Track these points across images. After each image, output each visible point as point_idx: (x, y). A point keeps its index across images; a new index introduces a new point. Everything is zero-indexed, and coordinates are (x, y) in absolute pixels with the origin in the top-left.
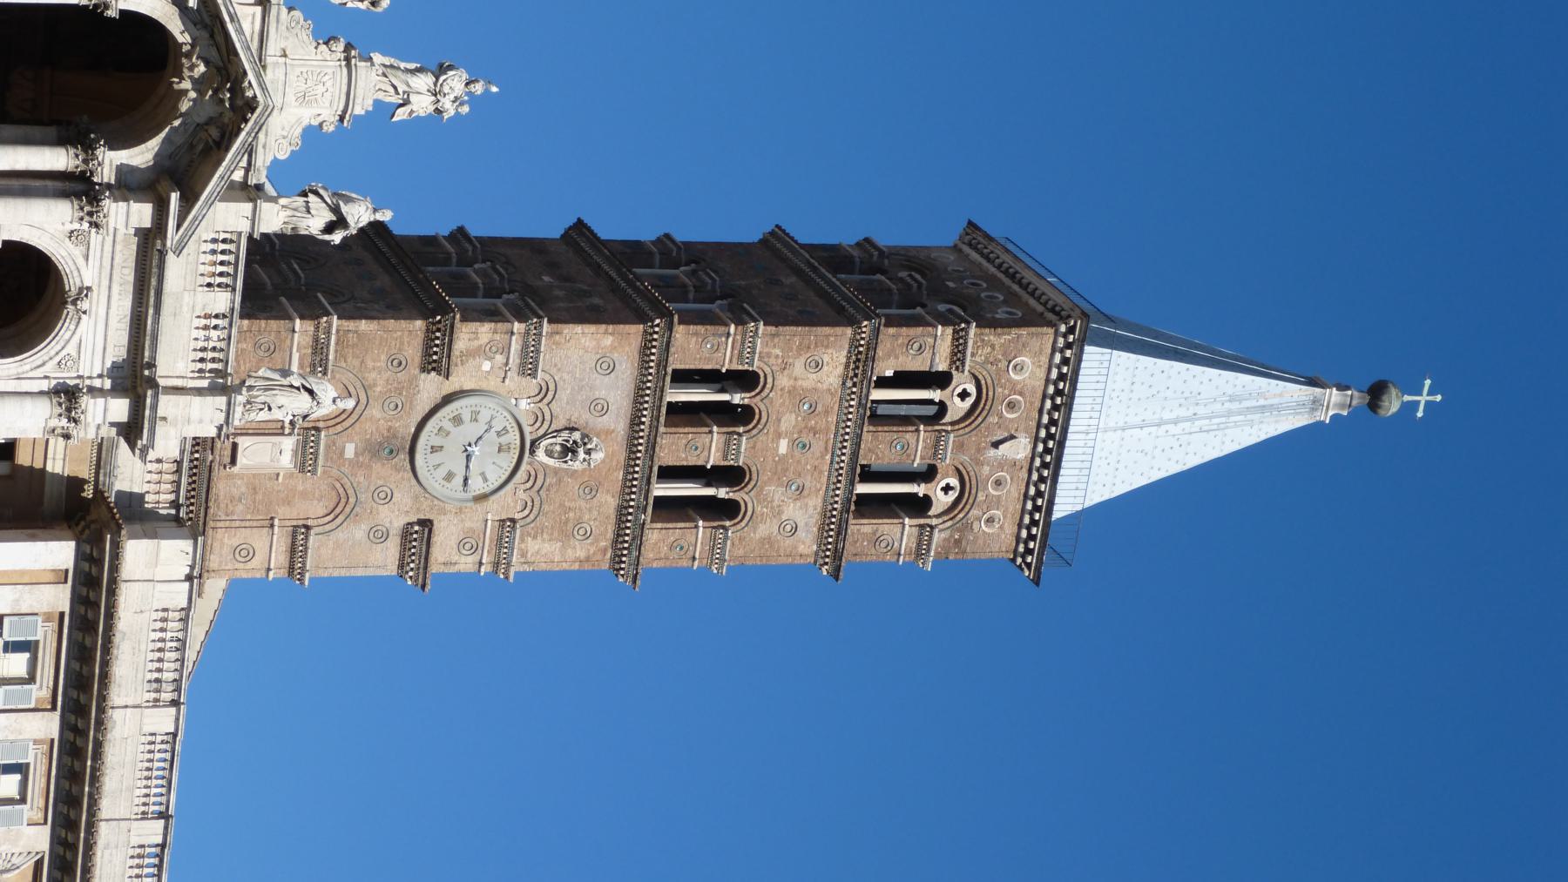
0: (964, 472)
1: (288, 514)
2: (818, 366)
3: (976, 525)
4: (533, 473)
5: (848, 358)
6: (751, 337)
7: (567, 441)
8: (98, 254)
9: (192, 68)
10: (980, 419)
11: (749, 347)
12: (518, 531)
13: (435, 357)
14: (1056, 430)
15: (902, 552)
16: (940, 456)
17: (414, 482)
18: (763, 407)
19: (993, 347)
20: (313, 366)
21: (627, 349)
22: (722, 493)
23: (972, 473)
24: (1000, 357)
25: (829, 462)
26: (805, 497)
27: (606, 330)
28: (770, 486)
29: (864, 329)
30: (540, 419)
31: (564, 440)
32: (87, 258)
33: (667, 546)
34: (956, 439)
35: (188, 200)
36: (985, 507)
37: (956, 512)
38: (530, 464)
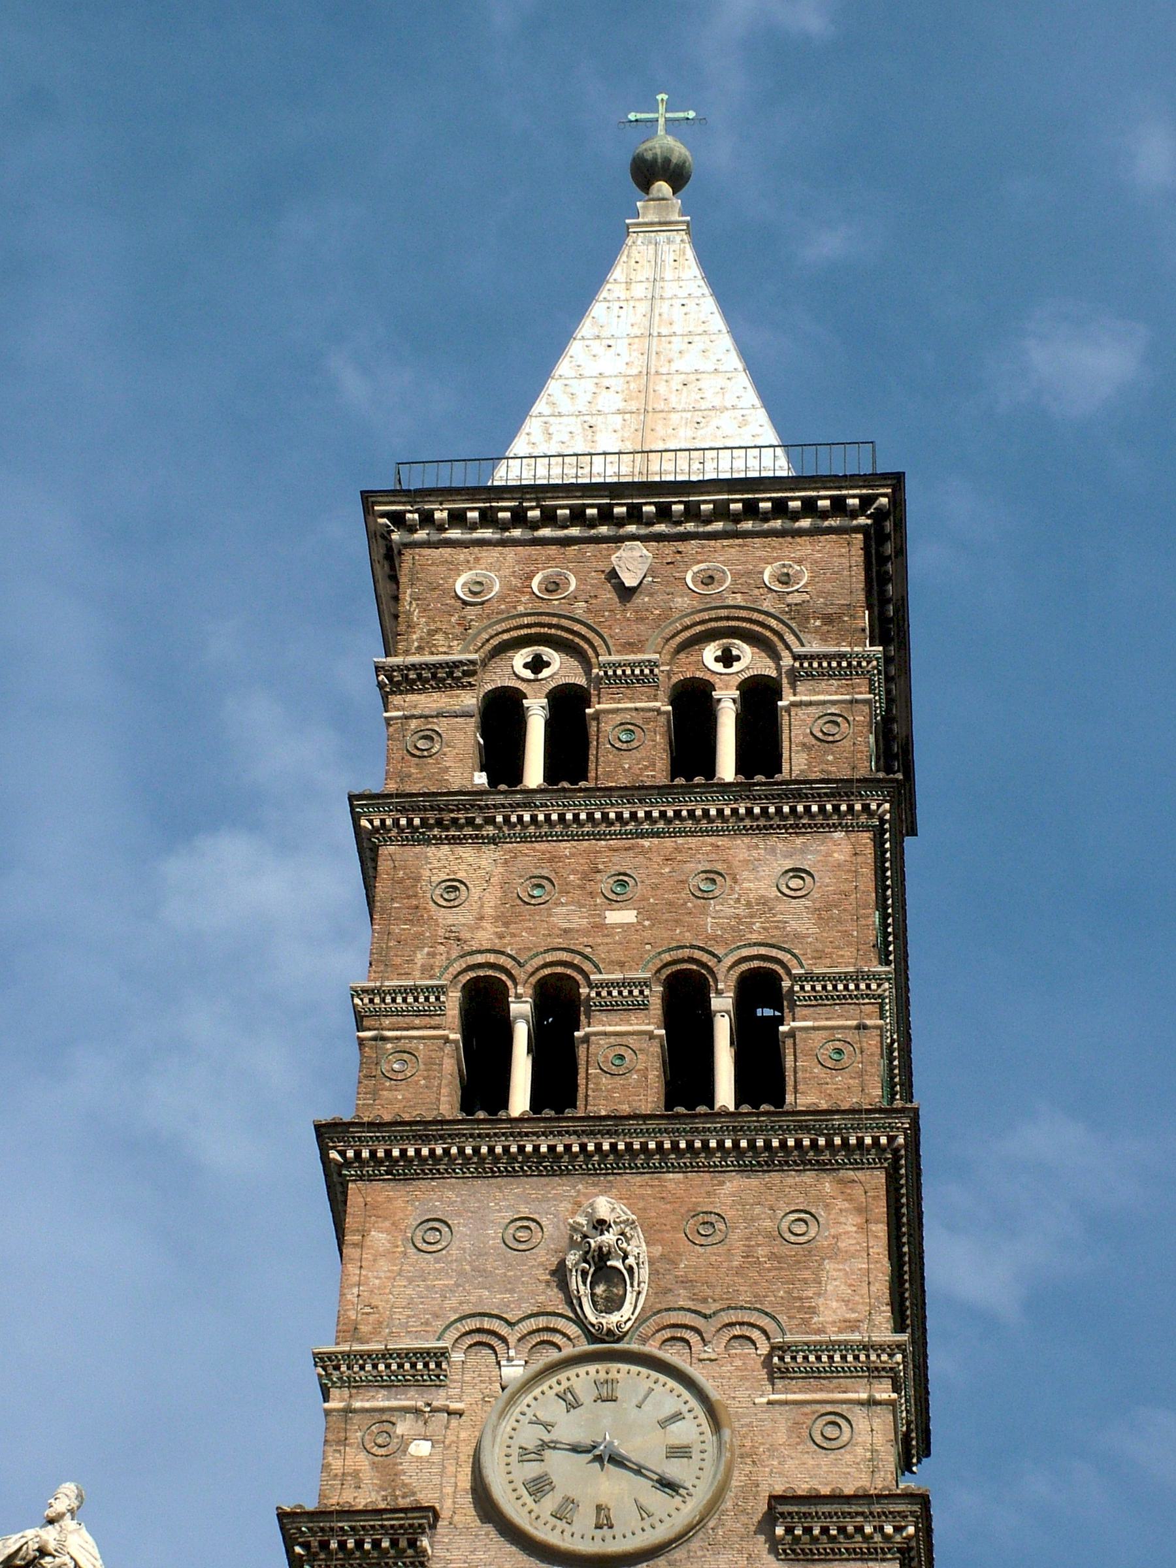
0: (687, 634)
2: (453, 886)
3: (796, 599)
4: (667, 1334)
5: (440, 841)
6: (383, 1000)
7: (584, 1274)
10: (577, 627)
11: (405, 1000)
12: (789, 1338)
13: (385, 1544)
14: (592, 506)
15: (848, 697)
16: (647, 671)
17: (678, 1554)
18: (538, 961)
19: (432, 633)
21: (399, 1203)
22: (722, 1003)
23: (687, 621)
24: (453, 619)
25: (656, 841)
26: (730, 868)
27: (355, 1245)
28: (706, 925)
29: (377, 823)
30: (546, 1336)
31: (584, 1283)
33: (832, 1077)
34: (612, 648)
36: (756, 592)
37: (768, 634)
38: (644, 1340)
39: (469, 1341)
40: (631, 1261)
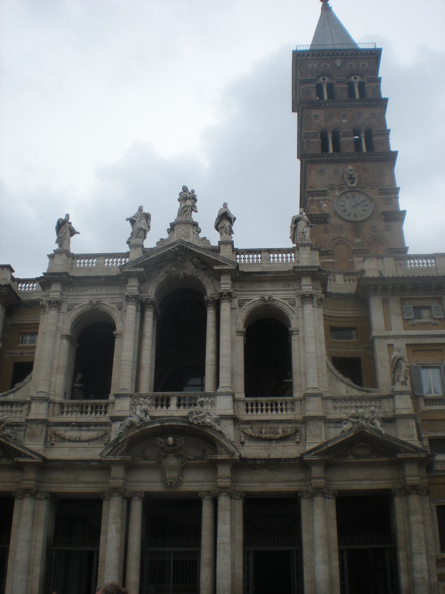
2: (316, 117)
8: (248, 296)
9: (174, 272)
20: (329, 255)
31: (348, 179)
32: (250, 300)
35: (218, 263)
39: (330, 189)
40: (355, 176)
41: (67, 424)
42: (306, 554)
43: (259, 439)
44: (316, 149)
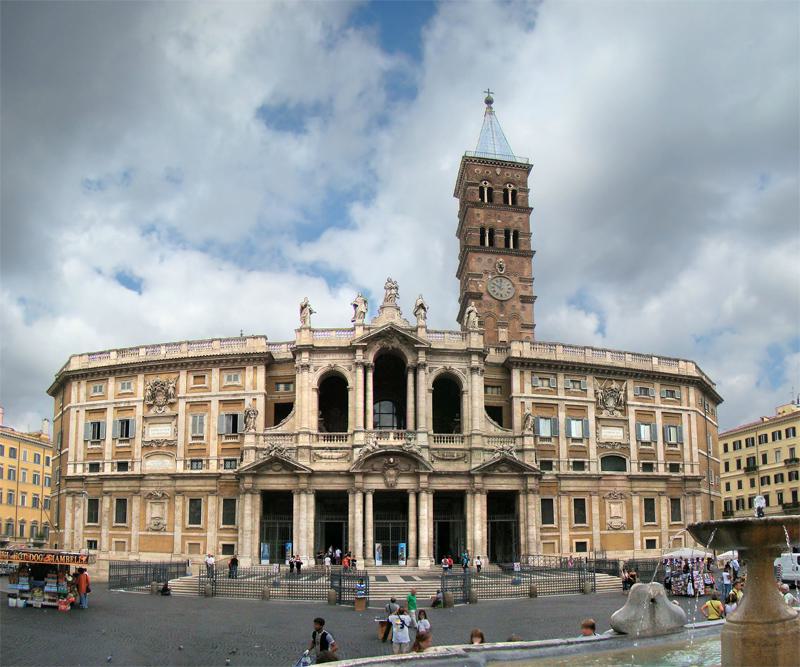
1: (519, 330)
41: (323, 448)
42: (469, 525)
43: (443, 460)
44: (477, 242)
